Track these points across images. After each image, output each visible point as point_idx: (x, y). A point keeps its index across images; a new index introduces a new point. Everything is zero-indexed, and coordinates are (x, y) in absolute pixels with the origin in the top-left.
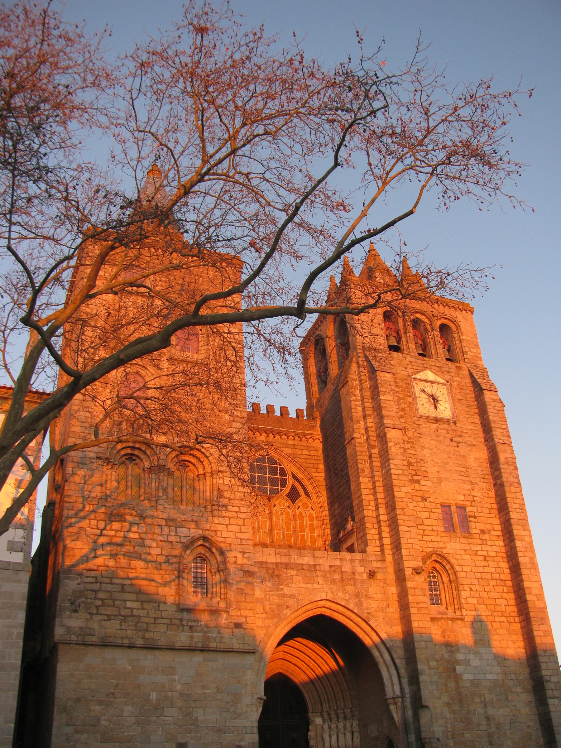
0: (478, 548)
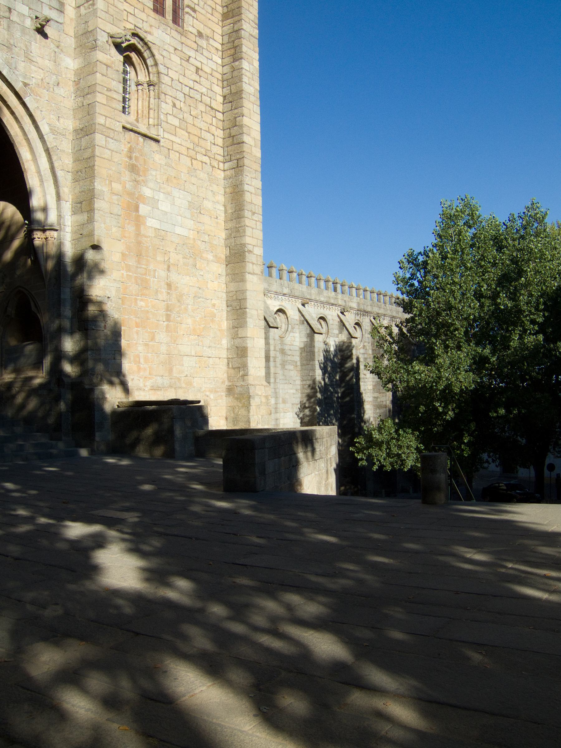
0: (192, 53)
